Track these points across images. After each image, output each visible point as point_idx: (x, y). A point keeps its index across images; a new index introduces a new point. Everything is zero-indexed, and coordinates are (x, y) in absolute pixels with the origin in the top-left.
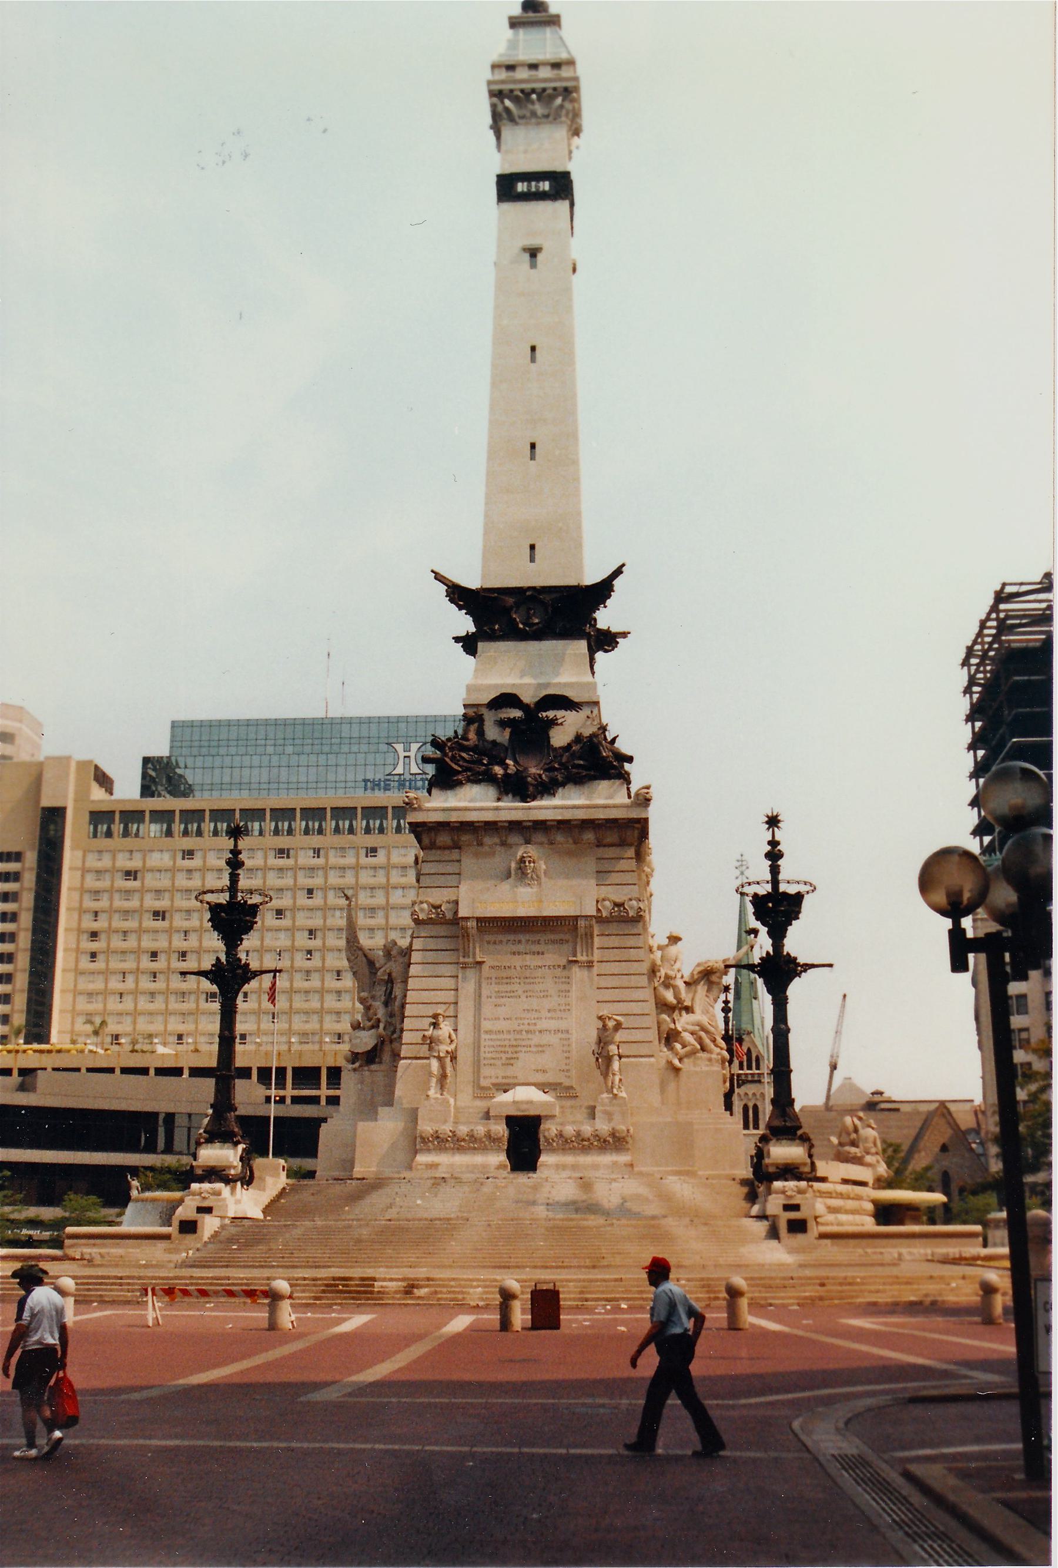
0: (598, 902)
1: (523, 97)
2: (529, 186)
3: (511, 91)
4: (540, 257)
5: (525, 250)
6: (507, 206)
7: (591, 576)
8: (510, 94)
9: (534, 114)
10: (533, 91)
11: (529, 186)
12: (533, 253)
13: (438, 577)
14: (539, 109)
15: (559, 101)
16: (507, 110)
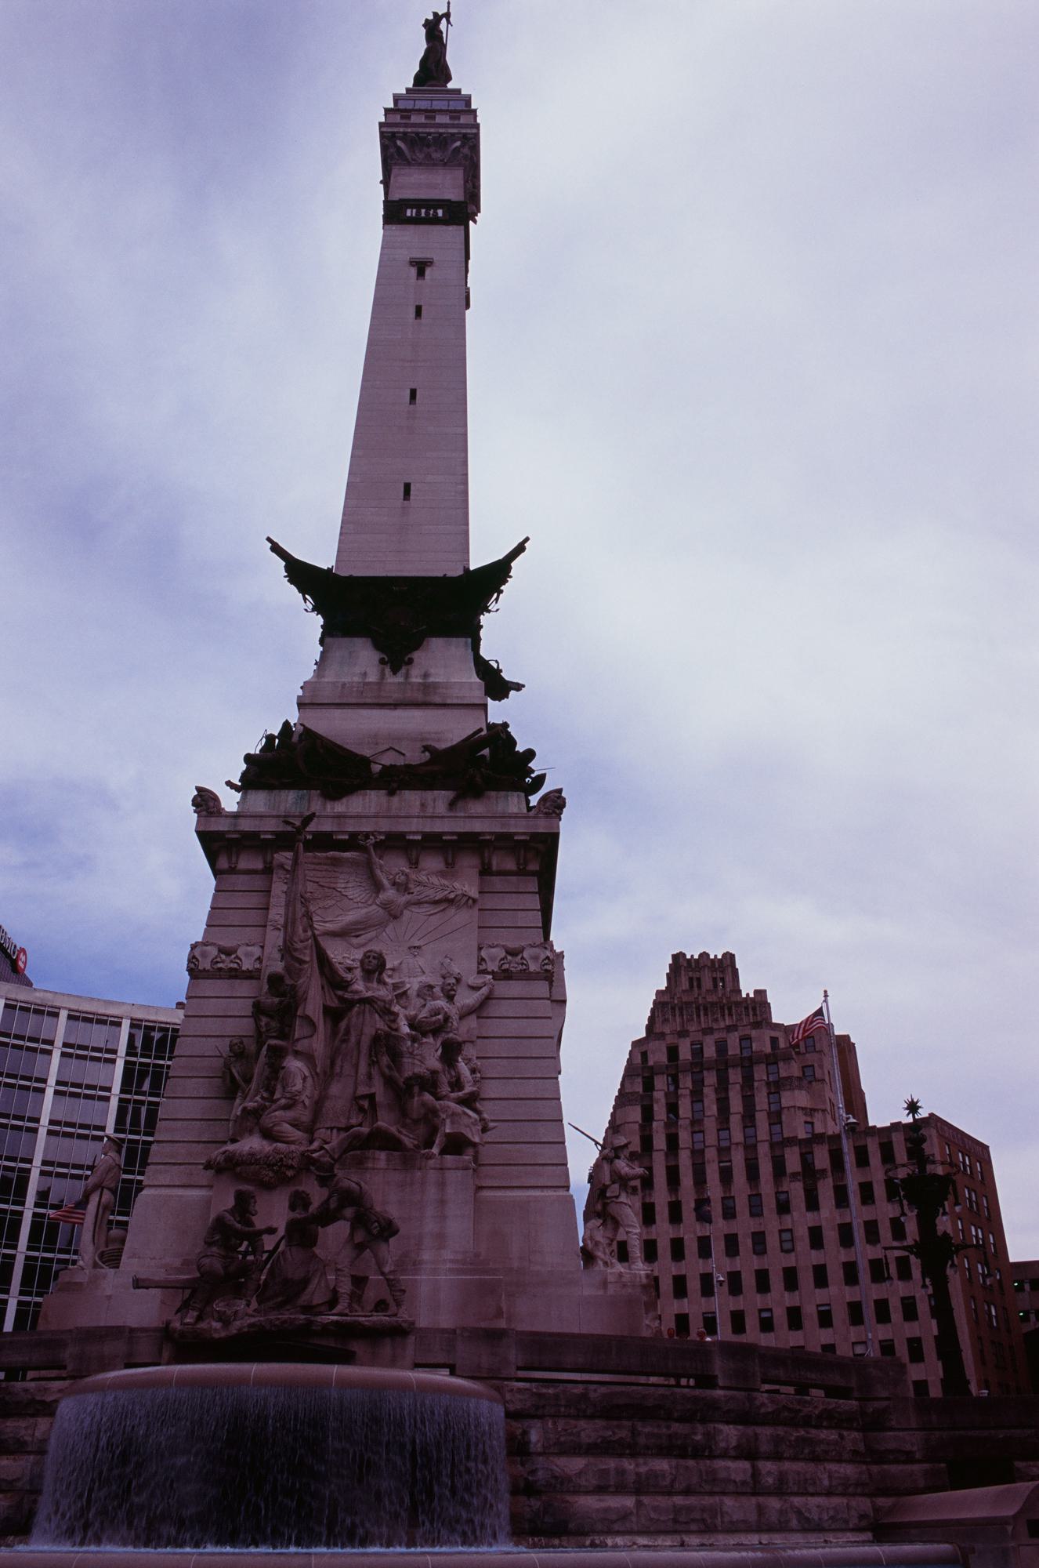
0: (480, 949)
1: (417, 141)
2: (418, 213)
3: (405, 134)
4: (428, 271)
5: (413, 263)
6: (394, 227)
7: (480, 558)
8: (405, 137)
9: (428, 156)
10: (429, 134)
11: (418, 213)
12: (421, 267)
13: (276, 549)
14: (436, 155)
15: (458, 144)
16: (399, 148)
